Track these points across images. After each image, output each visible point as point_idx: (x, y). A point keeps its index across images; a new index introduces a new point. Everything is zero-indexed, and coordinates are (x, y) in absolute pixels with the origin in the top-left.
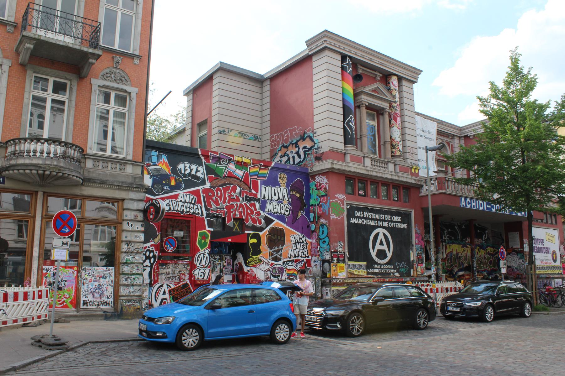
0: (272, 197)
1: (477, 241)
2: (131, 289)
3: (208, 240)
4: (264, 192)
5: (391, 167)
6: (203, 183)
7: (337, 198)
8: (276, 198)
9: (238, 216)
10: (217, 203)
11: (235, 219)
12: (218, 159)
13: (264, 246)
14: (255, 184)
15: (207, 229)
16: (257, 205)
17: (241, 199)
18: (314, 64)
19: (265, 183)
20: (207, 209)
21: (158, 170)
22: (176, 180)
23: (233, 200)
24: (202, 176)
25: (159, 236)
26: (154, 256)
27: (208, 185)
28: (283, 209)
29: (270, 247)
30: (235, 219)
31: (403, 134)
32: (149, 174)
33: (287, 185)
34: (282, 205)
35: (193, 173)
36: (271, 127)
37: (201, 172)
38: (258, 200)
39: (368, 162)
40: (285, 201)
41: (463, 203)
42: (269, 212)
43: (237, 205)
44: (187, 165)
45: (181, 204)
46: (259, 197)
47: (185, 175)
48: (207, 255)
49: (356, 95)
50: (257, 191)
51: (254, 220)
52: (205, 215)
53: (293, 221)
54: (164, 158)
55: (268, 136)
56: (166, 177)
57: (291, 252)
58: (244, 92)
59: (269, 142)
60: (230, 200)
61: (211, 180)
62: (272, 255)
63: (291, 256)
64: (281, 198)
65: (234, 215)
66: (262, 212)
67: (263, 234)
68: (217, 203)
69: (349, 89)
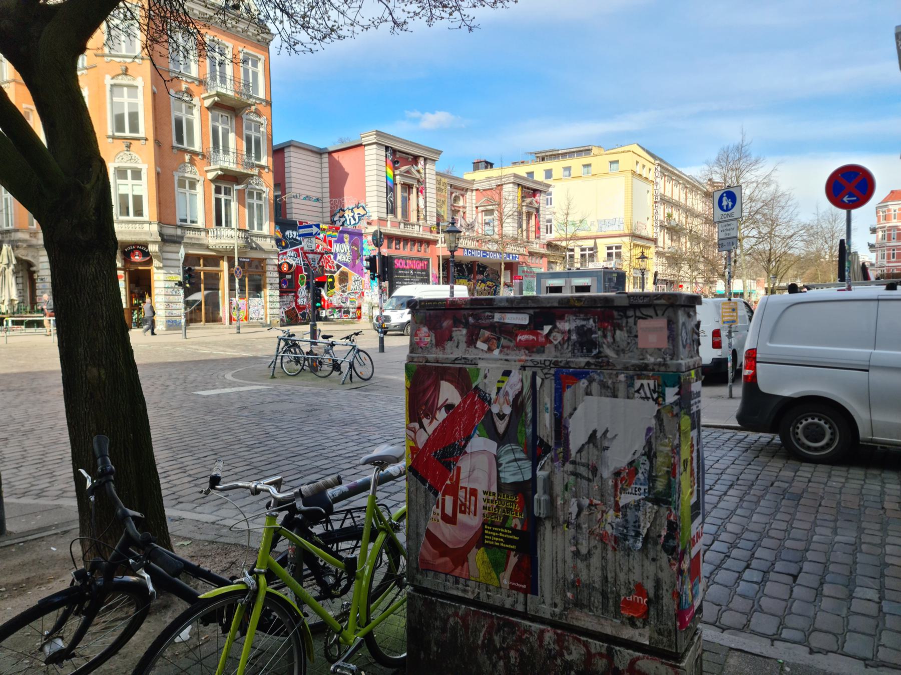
1: (479, 277)
2: (274, 310)
13: (337, 284)
14: (330, 242)
16: (332, 256)
18: (366, 153)
19: (336, 242)
28: (347, 258)
31: (426, 202)
36: (331, 192)
49: (394, 176)
53: (353, 266)
55: (328, 200)
58: (309, 163)
59: (328, 205)
67: (336, 275)
69: (390, 172)
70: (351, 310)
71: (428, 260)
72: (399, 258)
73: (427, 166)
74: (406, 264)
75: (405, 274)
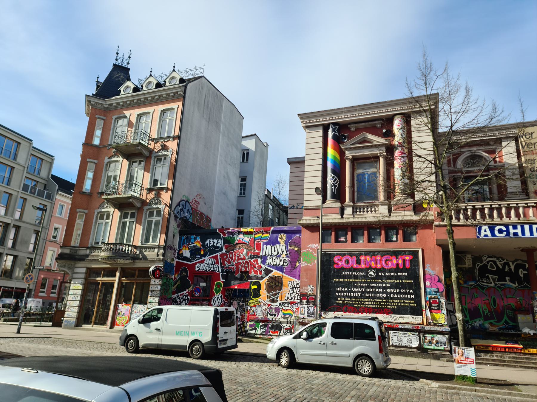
0: (272, 253)
3: (221, 288)
4: (265, 250)
5: (383, 209)
6: (221, 250)
7: (308, 248)
8: (276, 253)
9: (244, 269)
10: (229, 262)
11: (241, 272)
12: (232, 233)
13: (263, 292)
15: (221, 280)
16: (259, 260)
17: (246, 257)
19: (267, 244)
20: (222, 267)
21: (194, 246)
22: (204, 251)
23: (241, 259)
24: (220, 246)
25: (192, 287)
26: (188, 299)
27: (224, 250)
29: (268, 292)
30: (241, 272)
32: (189, 249)
33: (286, 243)
34: (281, 258)
35: (215, 245)
37: (220, 243)
38: (259, 257)
39: (348, 211)
40: (284, 255)
41: (488, 233)
42: (269, 265)
43: (243, 262)
44: (211, 240)
45: (206, 265)
46: (261, 254)
47: (210, 247)
48: (220, 298)
50: (259, 250)
51: (256, 272)
52: (220, 271)
54: (198, 239)
56: (199, 250)
57: (289, 296)
60: (239, 259)
61: (226, 248)
62: (270, 297)
63: (288, 298)
64: (280, 253)
65: (241, 269)
66: (263, 266)
67: (264, 282)
68: (229, 262)
69: (331, 152)
70: (284, 325)
71: (415, 254)
72: (342, 254)
73: (413, 122)
74: (358, 262)
75: (356, 277)
